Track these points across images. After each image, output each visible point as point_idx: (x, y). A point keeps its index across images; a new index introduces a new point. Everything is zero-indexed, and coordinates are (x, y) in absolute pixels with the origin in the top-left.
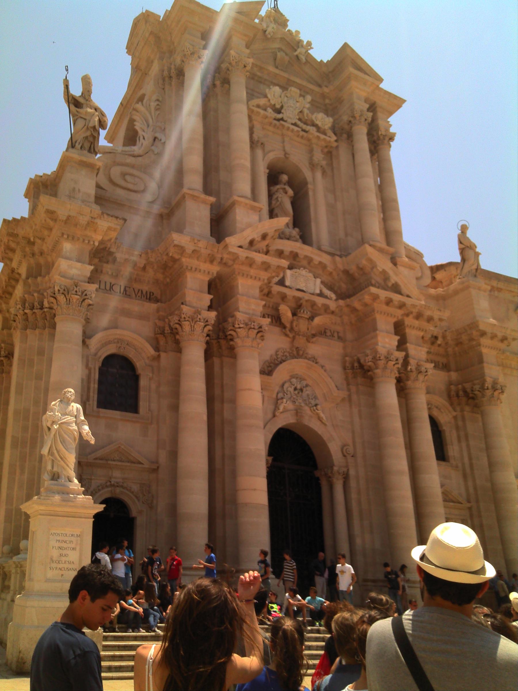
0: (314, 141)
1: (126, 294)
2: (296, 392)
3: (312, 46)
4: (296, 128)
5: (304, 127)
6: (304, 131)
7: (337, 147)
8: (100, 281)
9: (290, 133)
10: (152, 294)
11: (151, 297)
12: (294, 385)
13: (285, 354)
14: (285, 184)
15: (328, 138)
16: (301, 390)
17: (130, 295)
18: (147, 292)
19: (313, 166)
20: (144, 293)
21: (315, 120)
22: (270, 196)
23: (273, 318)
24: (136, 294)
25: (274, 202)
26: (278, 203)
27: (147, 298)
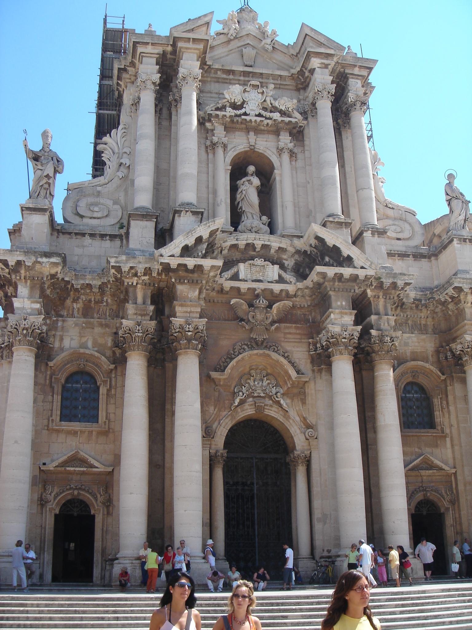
4: (259, 119)
5: (268, 114)
12: (253, 377)
14: (252, 175)
15: (293, 120)
19: (280, 151)
21: (278, 106)
22: (234, 189)
25: (238, 196)
26: (243, 196)
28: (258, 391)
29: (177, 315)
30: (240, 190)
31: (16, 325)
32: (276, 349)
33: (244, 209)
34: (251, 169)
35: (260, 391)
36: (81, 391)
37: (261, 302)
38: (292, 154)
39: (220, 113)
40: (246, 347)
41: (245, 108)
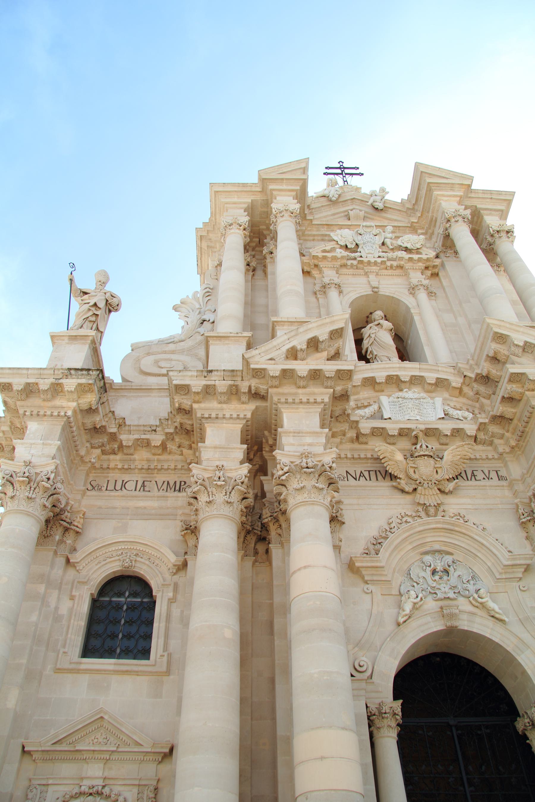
0: (408, 265)
1: (144, 490)
2: (437, 577)
3: (387, 191)
4: (379, 260)
6: (389, 260)
7: (443, 265)
8: (108, 481)
9: (375, 268)
10: (183, 483)
11: (182, 487)
13: (404, 520)
15: (424, 257)
16: (446, 572)
17: (149, 491)
18: (175, 482)
19: (413, 290)
20: (172, 484)
23: (378, 473)
24: (159, 488)
26: (372, 340)
27: (175, 491)
28: (443, 590)
29: (286, 448)
30: (365, 336)
31: (11, 476)
32: (461, 519)
33: (375, 353)
34: (379, 314)
35: (447, 590)
36: (125, 607)
37: (424, 447)
38: (431, 294)
39: (329, 255)
40: (409, 519)
41: (360, 252)
